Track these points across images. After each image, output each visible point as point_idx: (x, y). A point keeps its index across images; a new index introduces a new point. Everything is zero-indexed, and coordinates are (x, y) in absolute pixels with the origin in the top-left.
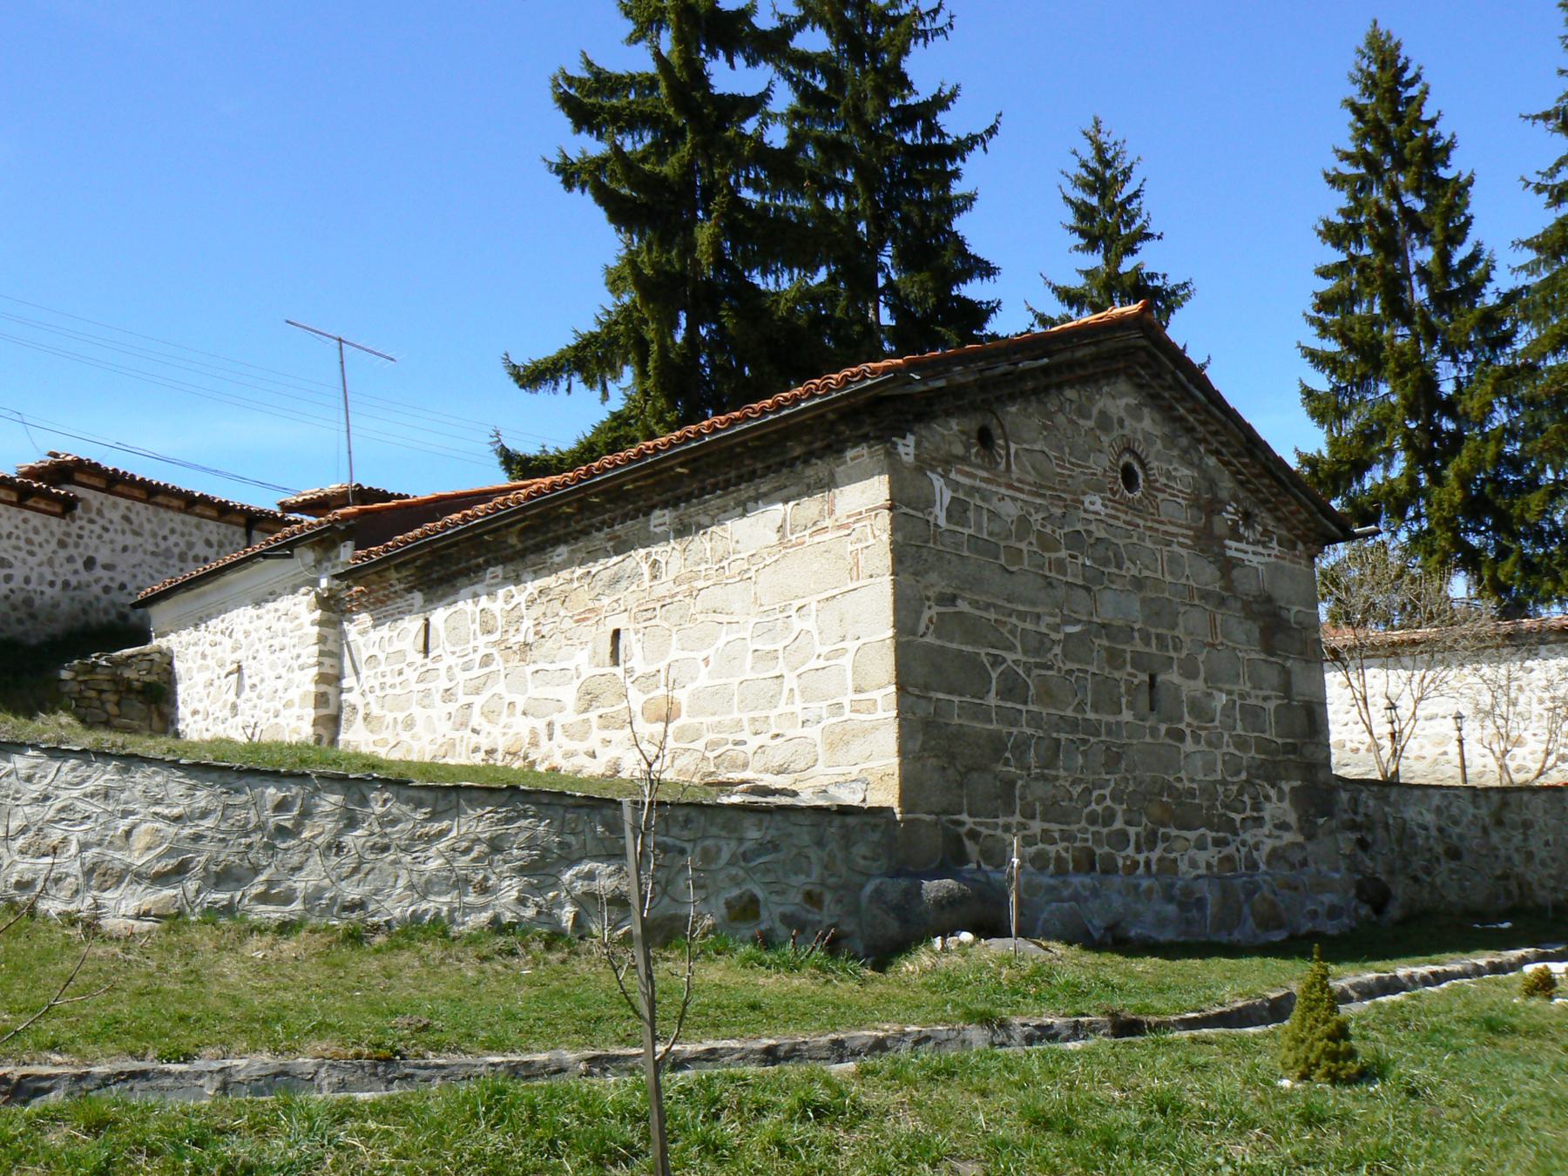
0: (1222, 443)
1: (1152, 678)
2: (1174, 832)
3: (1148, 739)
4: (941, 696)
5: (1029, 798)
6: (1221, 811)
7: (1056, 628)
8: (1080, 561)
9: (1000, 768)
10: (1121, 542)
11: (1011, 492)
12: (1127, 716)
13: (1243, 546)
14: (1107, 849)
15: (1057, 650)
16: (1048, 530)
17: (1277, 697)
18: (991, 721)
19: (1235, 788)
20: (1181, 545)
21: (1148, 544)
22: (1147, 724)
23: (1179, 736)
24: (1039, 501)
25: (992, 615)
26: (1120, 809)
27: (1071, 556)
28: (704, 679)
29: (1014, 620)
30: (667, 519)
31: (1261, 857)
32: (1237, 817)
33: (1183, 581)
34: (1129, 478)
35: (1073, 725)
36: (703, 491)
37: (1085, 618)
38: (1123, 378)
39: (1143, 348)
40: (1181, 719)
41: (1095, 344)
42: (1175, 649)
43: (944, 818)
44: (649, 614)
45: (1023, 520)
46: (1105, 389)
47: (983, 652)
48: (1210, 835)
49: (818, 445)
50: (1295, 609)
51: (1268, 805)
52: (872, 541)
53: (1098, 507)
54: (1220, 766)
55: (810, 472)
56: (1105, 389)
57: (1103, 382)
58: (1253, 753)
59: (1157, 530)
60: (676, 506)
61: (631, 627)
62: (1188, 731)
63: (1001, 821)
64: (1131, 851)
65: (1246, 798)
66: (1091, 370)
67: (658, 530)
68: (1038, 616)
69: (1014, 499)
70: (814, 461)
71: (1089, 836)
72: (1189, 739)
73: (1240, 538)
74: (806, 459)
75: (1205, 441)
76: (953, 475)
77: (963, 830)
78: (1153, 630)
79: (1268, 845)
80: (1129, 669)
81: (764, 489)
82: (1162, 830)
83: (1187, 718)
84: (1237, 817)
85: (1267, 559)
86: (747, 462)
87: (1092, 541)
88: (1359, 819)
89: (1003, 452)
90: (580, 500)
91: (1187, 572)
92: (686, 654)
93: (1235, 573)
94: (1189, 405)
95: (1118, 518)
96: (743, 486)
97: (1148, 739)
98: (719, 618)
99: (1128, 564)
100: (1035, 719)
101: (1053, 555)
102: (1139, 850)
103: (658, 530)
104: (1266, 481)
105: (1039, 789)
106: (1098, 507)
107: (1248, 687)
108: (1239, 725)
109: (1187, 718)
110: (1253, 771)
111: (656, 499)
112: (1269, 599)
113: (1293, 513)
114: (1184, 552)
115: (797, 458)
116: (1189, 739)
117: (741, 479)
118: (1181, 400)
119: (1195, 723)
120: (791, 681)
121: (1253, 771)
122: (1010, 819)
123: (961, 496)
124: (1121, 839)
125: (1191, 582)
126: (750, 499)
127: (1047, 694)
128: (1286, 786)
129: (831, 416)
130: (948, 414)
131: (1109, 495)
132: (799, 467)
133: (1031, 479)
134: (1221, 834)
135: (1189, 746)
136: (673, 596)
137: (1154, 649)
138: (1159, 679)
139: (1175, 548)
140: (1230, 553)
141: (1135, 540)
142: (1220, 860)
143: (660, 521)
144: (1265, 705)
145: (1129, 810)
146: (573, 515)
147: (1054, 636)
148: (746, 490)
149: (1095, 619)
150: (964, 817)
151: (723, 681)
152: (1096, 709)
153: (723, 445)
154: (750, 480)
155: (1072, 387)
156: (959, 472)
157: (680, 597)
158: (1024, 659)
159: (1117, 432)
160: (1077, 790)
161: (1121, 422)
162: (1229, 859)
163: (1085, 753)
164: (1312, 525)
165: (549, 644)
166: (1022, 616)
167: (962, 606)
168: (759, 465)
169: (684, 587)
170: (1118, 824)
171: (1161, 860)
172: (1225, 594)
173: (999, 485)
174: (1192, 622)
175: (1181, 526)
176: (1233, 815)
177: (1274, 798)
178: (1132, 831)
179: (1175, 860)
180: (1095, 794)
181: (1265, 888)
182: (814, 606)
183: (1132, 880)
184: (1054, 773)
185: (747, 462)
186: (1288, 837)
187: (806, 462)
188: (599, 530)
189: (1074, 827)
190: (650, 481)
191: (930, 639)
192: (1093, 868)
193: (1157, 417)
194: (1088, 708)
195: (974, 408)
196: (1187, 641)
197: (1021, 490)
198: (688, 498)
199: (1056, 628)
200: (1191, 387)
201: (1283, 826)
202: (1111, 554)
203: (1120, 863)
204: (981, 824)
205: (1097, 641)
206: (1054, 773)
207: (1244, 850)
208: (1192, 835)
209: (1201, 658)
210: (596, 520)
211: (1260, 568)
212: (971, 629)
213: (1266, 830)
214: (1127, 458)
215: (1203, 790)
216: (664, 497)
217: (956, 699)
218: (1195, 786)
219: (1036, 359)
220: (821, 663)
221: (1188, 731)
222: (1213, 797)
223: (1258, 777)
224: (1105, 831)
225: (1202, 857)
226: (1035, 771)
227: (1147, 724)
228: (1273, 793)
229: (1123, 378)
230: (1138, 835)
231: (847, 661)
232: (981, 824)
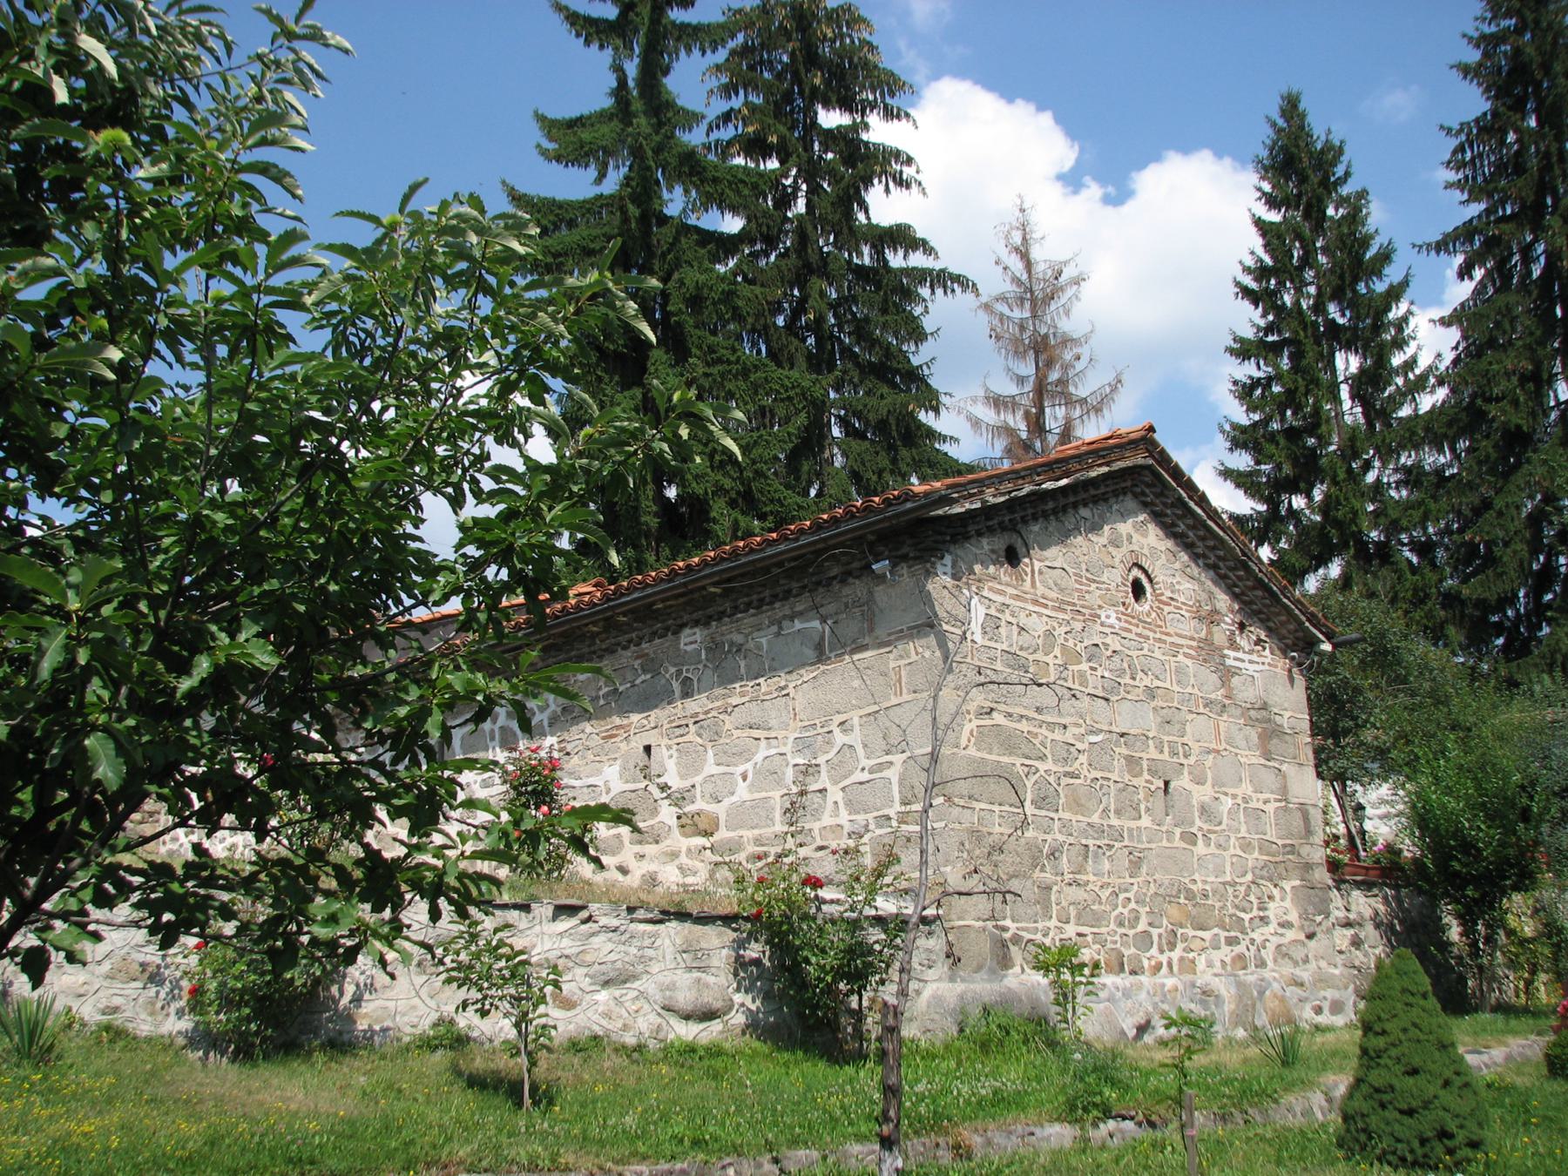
0: (1219, 558)
1: (1167, 783)
2: (1191, 932)
3: (1165, 843)
4: (983, 806)
5: (1064, 904)
6: (1232, 911)
7: (1081, 738)
8: (1099, 673)
9: (1037, 874)
10: (1134, 654)
11: (1037, 609)
12: (1145, 821)
13: (1240, 655)
14: (1133, 950)
16: (1071, 643)
17: (1277, 800)
19: (1242, 889)
20: (1185, 655)
21: (1157, 654)
22: (1164, 829)
23: (1190, 838)
24: (1061, 616)
25: (1024, 726)
26: (1143, 910)
27: (1092, 669)
28: (743, 792)
29: (1043, 731)
30: (698, 637)
31: (1268, 955)
32: (1246, 917)
33: (1189, 690)
34: (1138, 590)
36: (736, 609)
37: (1105, 728)
38: (1129, 496)
39: (1149, 467)
40: (1192, 823)
41: (1107, 464)
42: (1186, 756)
43: (990, 924)
44: (680, 731)
45: (1049, 633)
46: (1115, 507)
47: (1018, 761)
48: (1223, 934)
49: (856, 565)
50: (1287, 714)
51: (1271, 905)
52: (914, 657)
53: (1112, 620)
54: (1228, 868)
55: (846, 591)
56: (1115, 507)
57: (1112, 500)
58: (1256, 854)
59: (1164, 642)
60: (707, 624)
61: (665, 741)
62: (1200, 835)
63: (1040, 925)
64: (1154, 951)
65: (1252, 898)
66: (1102, 490)
67: (689, 648)
68: (1065, 727)
69: (1040, 615)
70: (851, 580)
71: (1117, 938)
72: (1200, 842)
73: (1237, 648)
74: (844, 578)
75: (1204, 556)
76: (985, 593)
77: (1007, 935)
78: (1166, 738)
79: (1275, 940)
80: (1146, 776)
81: (799, 608)
82: (1181, 931)
83: (1198, 823)
84: (1246, 917)
86: (782, 582)
87: (1109, 653)
88: (1352, 916)
89: (1028, 570)
90: (606, 619)
91: (1192, 681)
92: (722, 769)
93: (1235, 680)
94: (1190, 522)
95: (1130, 631)
96: (777, 605)
97: (1165, 843)
98: (756, 734)
99: (1140, 675)
100: (1065, 826)
101: (1076, 668)
102: (1162, 951)
103: (689, 648)
104: (1259, 593)
105: (1075, 893)
106: (1112, 620)
107: (1249, 790)
108: (1243, 828)
109: (1198, 823)
110: (1257, 872)
111: (686, 618)
112: (1265, 707)
113: (1282, 624)
114: (1189, 662)
115: (834, 578)
117: (775, 597)
118: (1180, 517)
119: (1205, 827)
120: (835, 794)
121: (1257, 872)
122: (1048, 924)
123: (993, 612)
124: (1145, 940)
125: (1196, 691)
126: (785, 617)
127: (1077, 805)
128: (1287, 885)
129: (871, 537)
130: (979, 534)
131: (1122, 609)
132: (836, 586)
133: (1053, 595)
134: (1233, 934)
135: (1200, 848)
136: (707, 713)
137: (1166, 756)
138: (1172, 785)
139: (1180, 657)
140: (1229, 662)
141: (1145, 652)
142: (1233, 960)
143: (688, 640)
145: (1151, 912)
146: (598, 634)
147: (1080, 746)
148: (781, 609)
149: (1114, 728)
150: (1008, 923)
151: (764, 794)
152: (1118, 812)
153: (759, 565)
154: (785, 599)
155: (1085, 505)
156: (991, 589)
157: (714, 713)
158: (1055, 769)
159: (1124, 550)
160: (1105, 894)
161: (1130, 537)
162: (1241, 957)
164: (1300, 634)
165: (575, 760)
166: (1051, 726)
167: (998, 718)
168: (795, 585)
169: (717, 704)
171: (1181, 959)
172: (1227, 702)
173: (1025, 600)
174: (1198, 729)
175: (1185, 637)
176: (1242, 915)
177: (1277, 897)
178: (1155, 932)
179: (1193, 961)
180: (1122, 896)
181: (1275, 985)
182: (856, 721)
183: (1158, 979)
184: (1084, 878)
185: (782, 582)
186: (1291, 935)
187: (843, 582)
188: (625, 648)
189: (1103, 930)
190: (681, 600)
191: (972, 751)
192: (1122, 969)
193: (1161, 533)
194: (1112, 815)
195: (1003, 528)
196: (1195, 747)
197: (1046, 606)
198: (720, 616)
199: (1081, 738)
200: (1192, 504)
201: (1285, 925)
202: (1125, 665)
203: (1146, 963)
204: (1023, 929)
205: (1117, 750)
206: (1084, 878)
208: (1207, 935)
209: (1208, 763)
210: (623, 639)
212: (1009, 743)
213: (1272, 928)
214: (1136, 572)
215: (1215, 892)
216: (695, 616)
217: (996, 808)
218: (1208, 887)
219: (1057, 480)
220: (866, 776)
221: (1200, 835)
222: (1223, 897)
224: (1131, 932)
225: (1216, 956)
226: (1068, 877)
227: (1164, 829)
228: (1276, 892)
229: (1129, 496)
230: (1160, 936)
231: (893, 774)
232: (1023, 929)
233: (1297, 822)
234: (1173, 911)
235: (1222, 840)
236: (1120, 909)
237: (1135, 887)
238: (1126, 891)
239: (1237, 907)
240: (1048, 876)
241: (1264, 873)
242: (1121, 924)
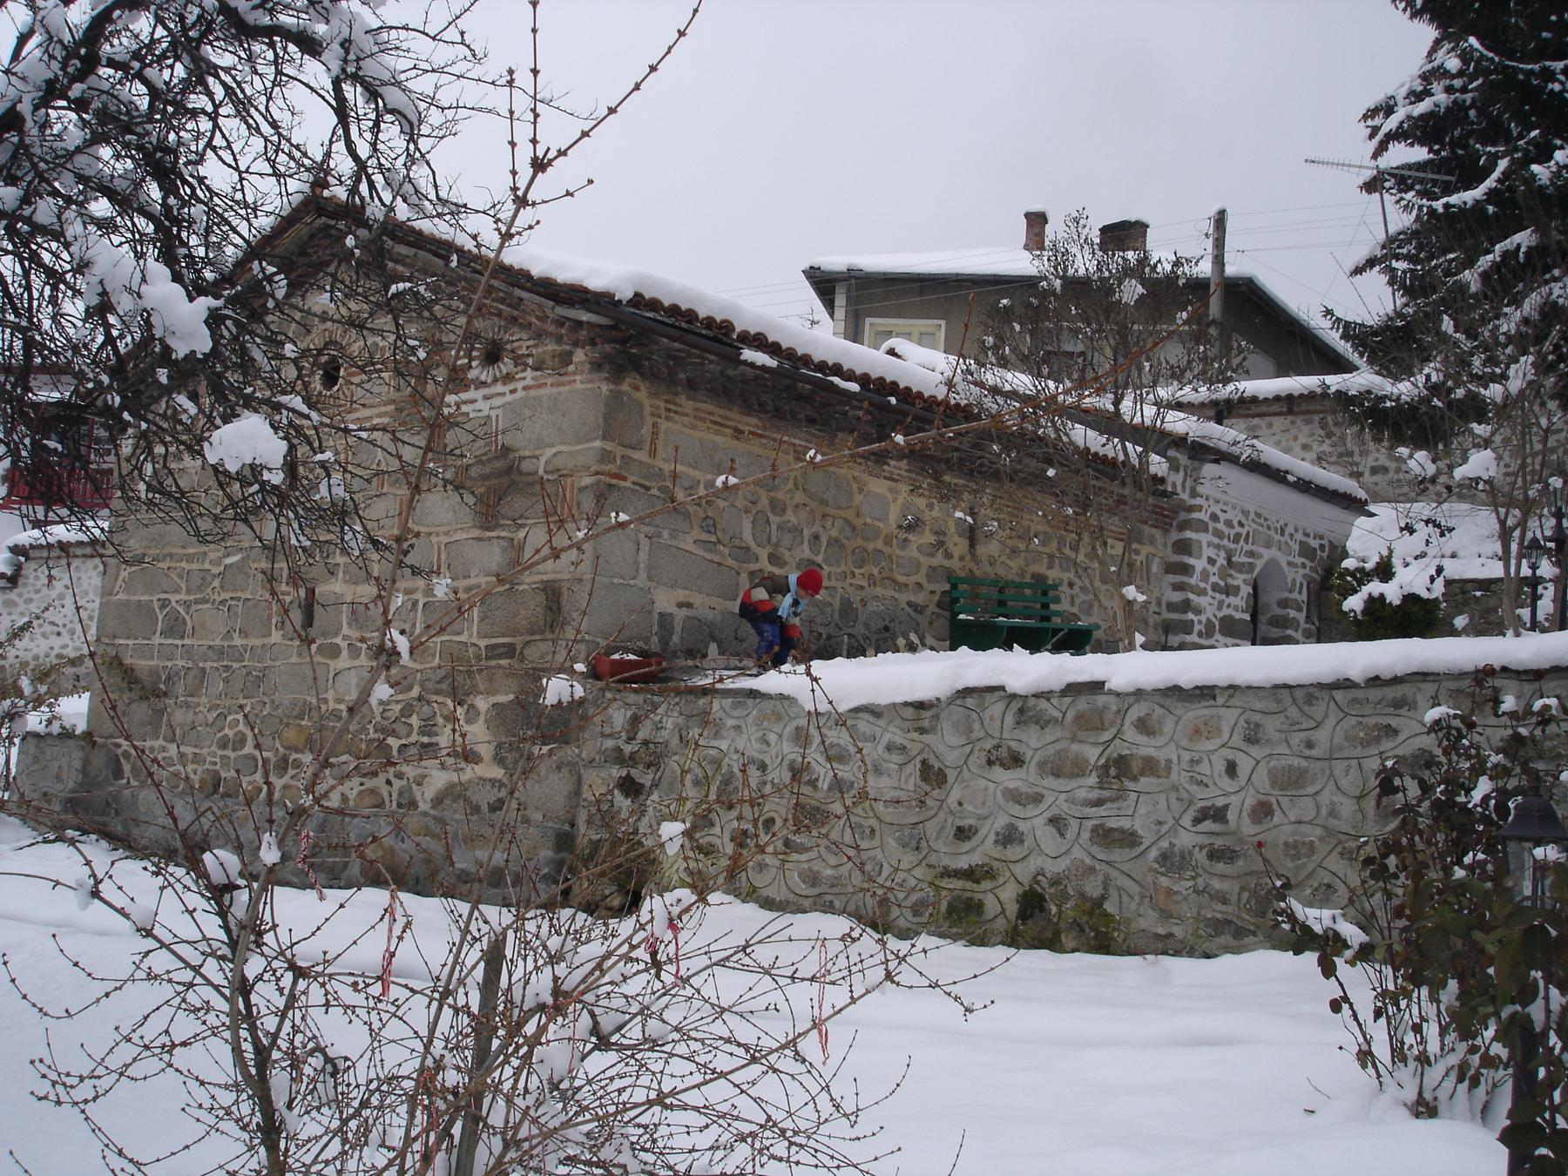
12: (276, 637)
15: (216, 583)
18: (152, 658)
35: (221, 653)
62: (344, 645)
72: (345, 653)
77: (119, 751)
82: (294, 756)
85: (509, 398)
109: (346, 630)
110: (430, 685)
163: (226, 680)
170: (249, 749)
184: (195, 700)
207: (397, 784)
211: (493, 414)
217: (130, 642)
223: (437, 693)
224: (233, 755)
233: (533, 608)
236: (226, 731)
239: (383, 730)
242: (224, 746)
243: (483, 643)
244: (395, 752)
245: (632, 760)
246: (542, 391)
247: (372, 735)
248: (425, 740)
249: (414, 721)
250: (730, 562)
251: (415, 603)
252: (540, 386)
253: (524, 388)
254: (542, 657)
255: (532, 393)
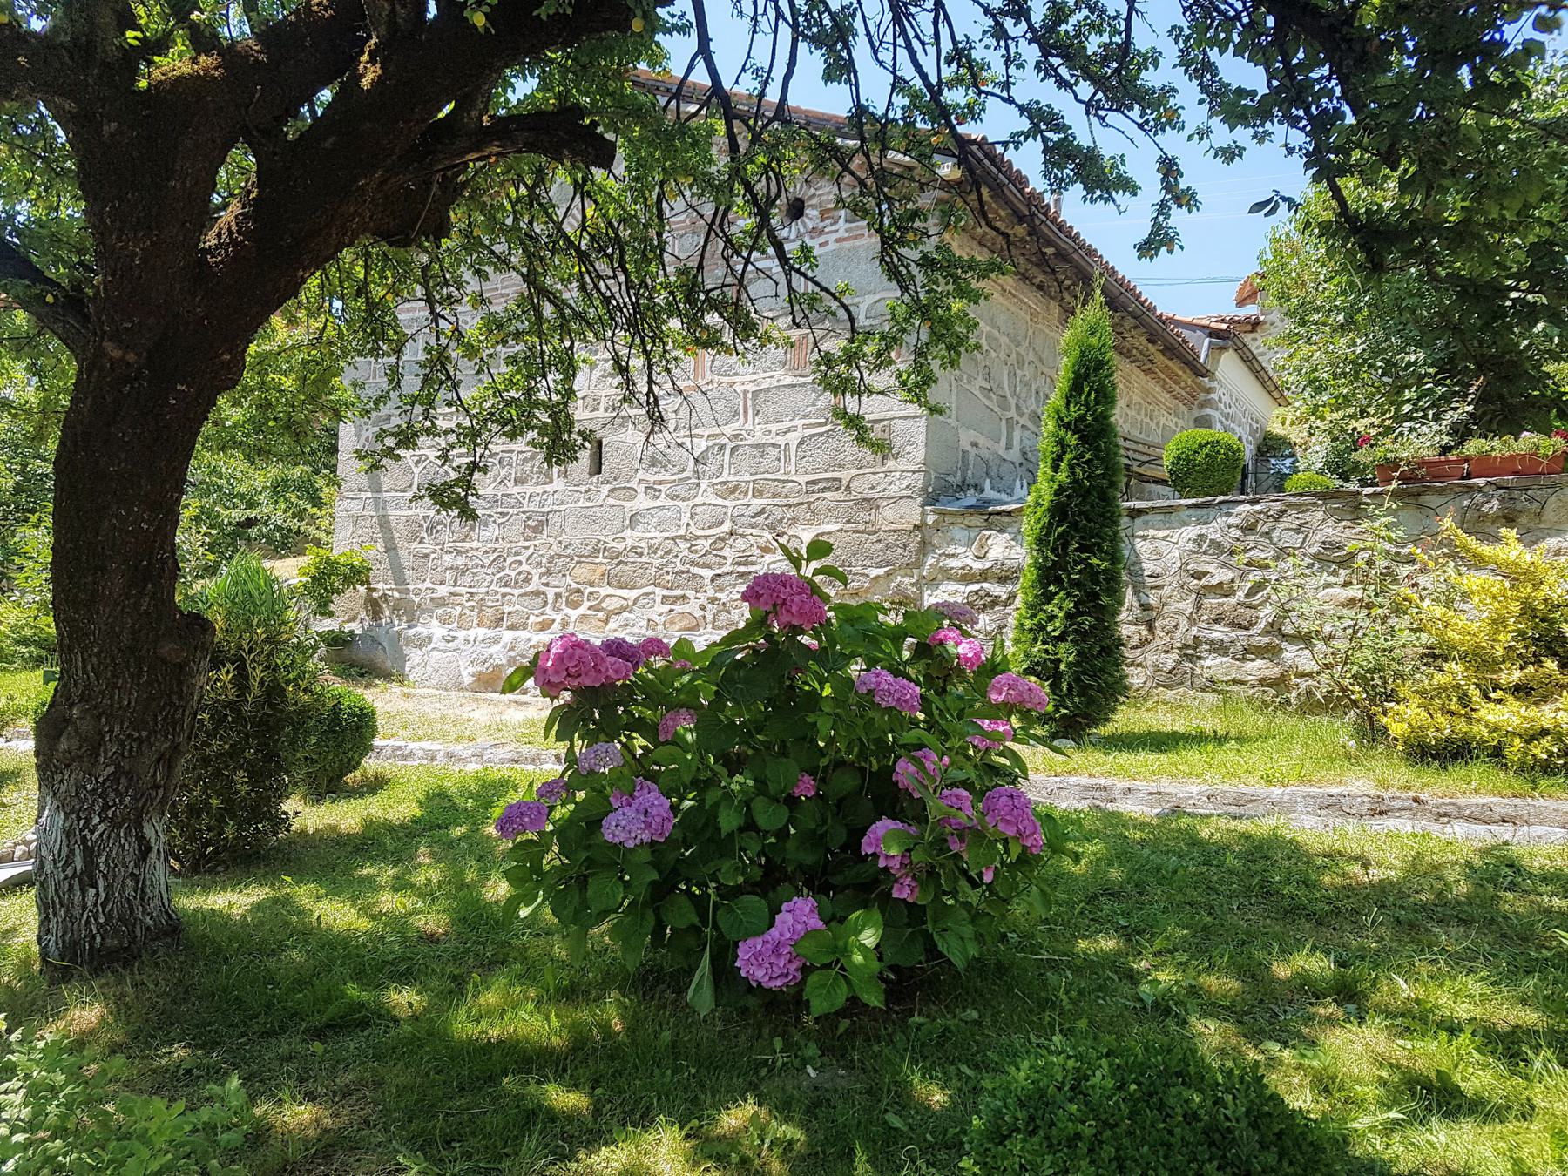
26: (535, 573)
32: (708, 574)
48: (660, 592)
64: (548, 609)
65: (727, 552)
72: (641, 495)
116: (641, 495)
144: (781, 441)
145: (549, 573)
180: (510, 560)
184: (467, 545)
218: (643, 544)
234: (584, 571)
235: (680, 490)
236: (507, 571)
237: (531, 550)
238: (517, 554)
240: (427, 547)
241: (760, 519)
243: (802, 479)
244: (707, 581)
245: (984, 576)
246: (857, 242)
247: (679, 567)
248: (742, 569)
249: (727, 552)
250: (996, 409)
251: (722, 447)
252: (856, 237)
253: (837, 241)
254: (872, 488)
255: (847, 244)
